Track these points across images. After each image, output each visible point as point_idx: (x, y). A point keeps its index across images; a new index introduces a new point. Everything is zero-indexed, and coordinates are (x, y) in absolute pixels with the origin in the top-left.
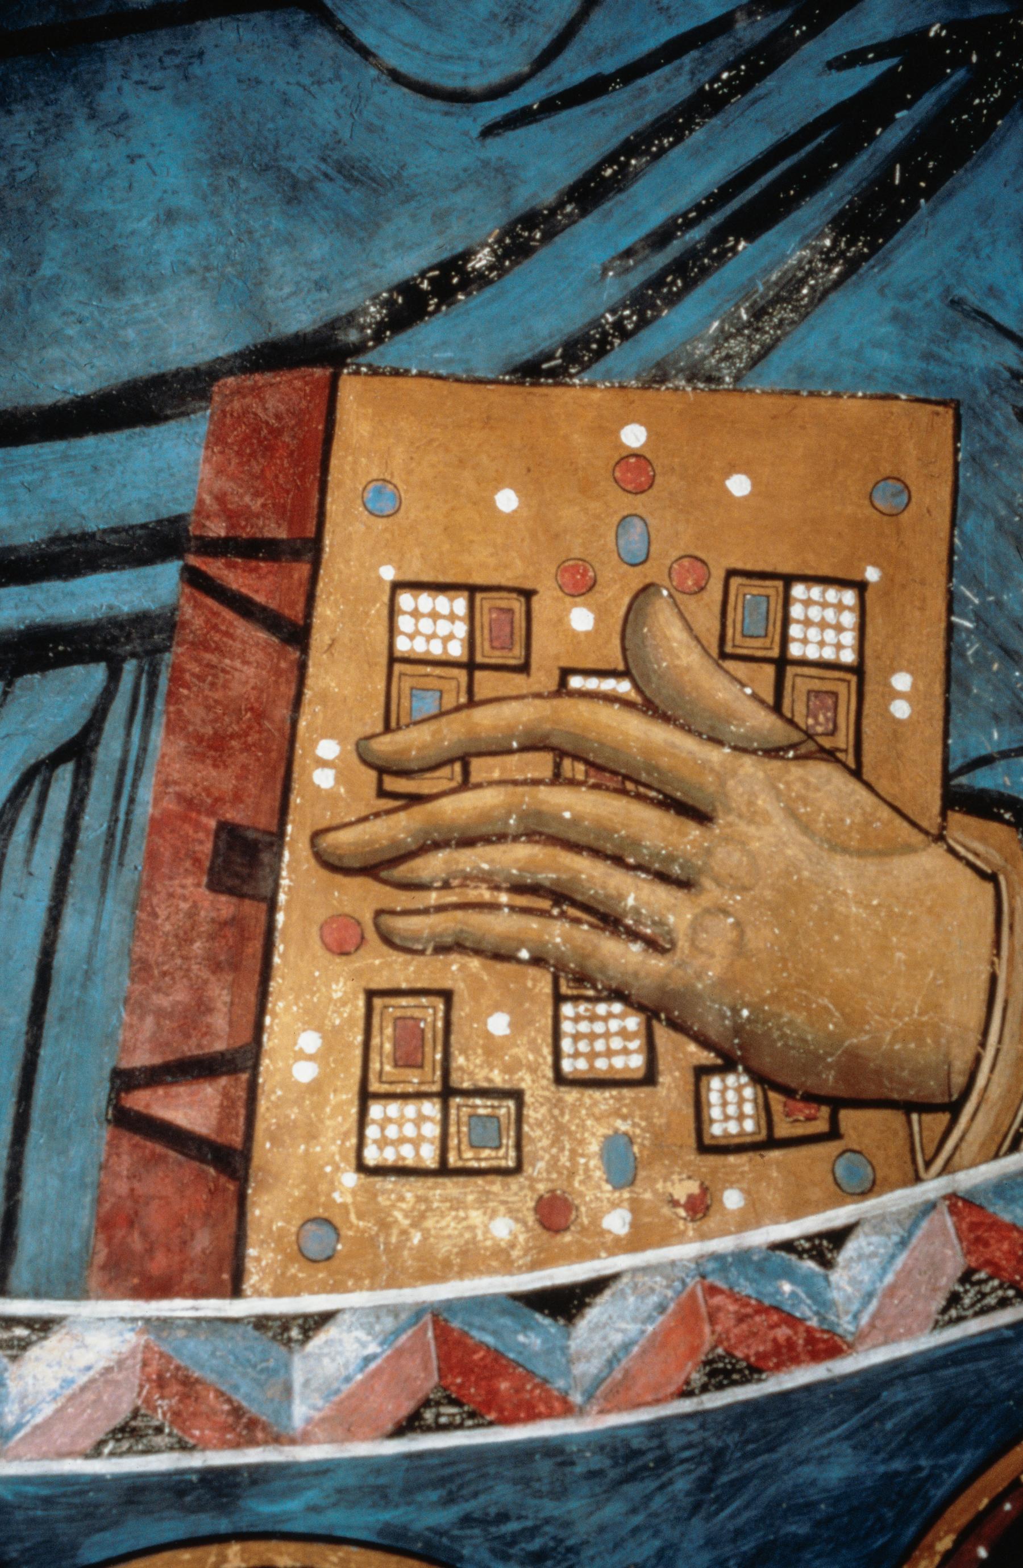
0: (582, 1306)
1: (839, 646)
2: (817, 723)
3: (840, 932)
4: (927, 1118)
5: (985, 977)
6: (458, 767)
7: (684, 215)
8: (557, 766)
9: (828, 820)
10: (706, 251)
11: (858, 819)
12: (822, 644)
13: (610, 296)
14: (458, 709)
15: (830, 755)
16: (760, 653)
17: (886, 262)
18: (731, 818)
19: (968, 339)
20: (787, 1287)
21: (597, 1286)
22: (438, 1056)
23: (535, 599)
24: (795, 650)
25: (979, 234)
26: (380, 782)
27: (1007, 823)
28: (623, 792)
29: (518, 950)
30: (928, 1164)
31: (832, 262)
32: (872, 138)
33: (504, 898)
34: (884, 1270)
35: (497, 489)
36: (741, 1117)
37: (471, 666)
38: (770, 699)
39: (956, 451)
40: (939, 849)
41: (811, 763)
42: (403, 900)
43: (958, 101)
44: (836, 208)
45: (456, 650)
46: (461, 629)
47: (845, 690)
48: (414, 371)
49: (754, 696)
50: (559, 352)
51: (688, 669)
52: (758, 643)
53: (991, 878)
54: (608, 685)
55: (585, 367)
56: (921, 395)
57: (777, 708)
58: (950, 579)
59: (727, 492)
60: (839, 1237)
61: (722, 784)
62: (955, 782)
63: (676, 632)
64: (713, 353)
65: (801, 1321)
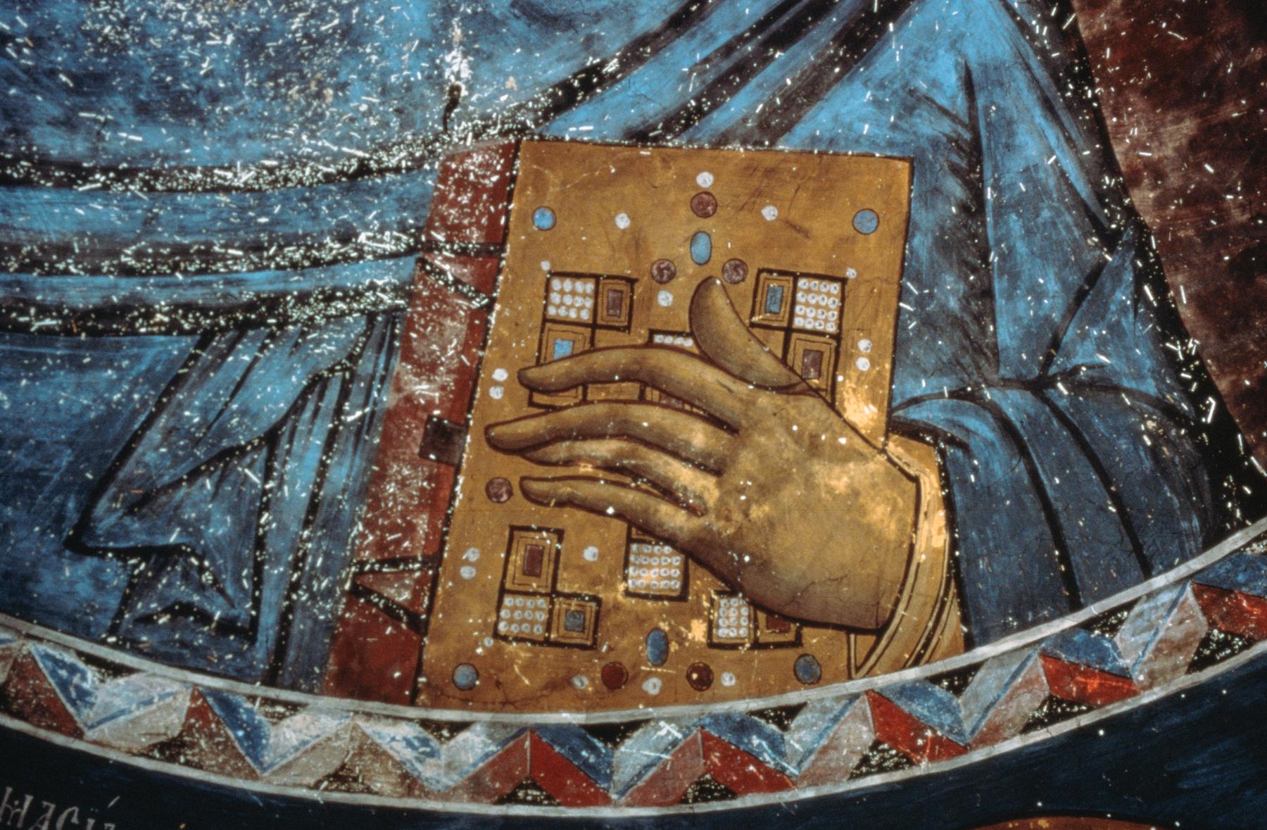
0: (624, 736)
1: (826, 321)
4: (860, 638)
6: (580, 389)
8: (642, 393)
13: (694, 88)
14: (584, 353)
15: (815, 392)
16: (775, 324)
19: (920, 116)
20: (756, 741)
21: (633, 726)
22: (551, 571)
23: (637, 285)
24: (798, 322)
26: (531, 397)
27: (928, 443)
28: (683, 411)
29: (607, 507)
30: (858, 669)
33: (601, 474)
34: (821, 736)
36: (739, 627)
37: (594, 326)
38: (779, 354)
39: (911, 191)
42: (539, 471)
44: (838, 29)
45: (585, 316)
46: (589, 303)
48: (567, 138)
49: (770, 352)
50: (661, 125)
54: (679, 341)
57: (783, 361)
58: (901, 278)
60: (793, 711)
62: (896, 414)
65: (763, 762)
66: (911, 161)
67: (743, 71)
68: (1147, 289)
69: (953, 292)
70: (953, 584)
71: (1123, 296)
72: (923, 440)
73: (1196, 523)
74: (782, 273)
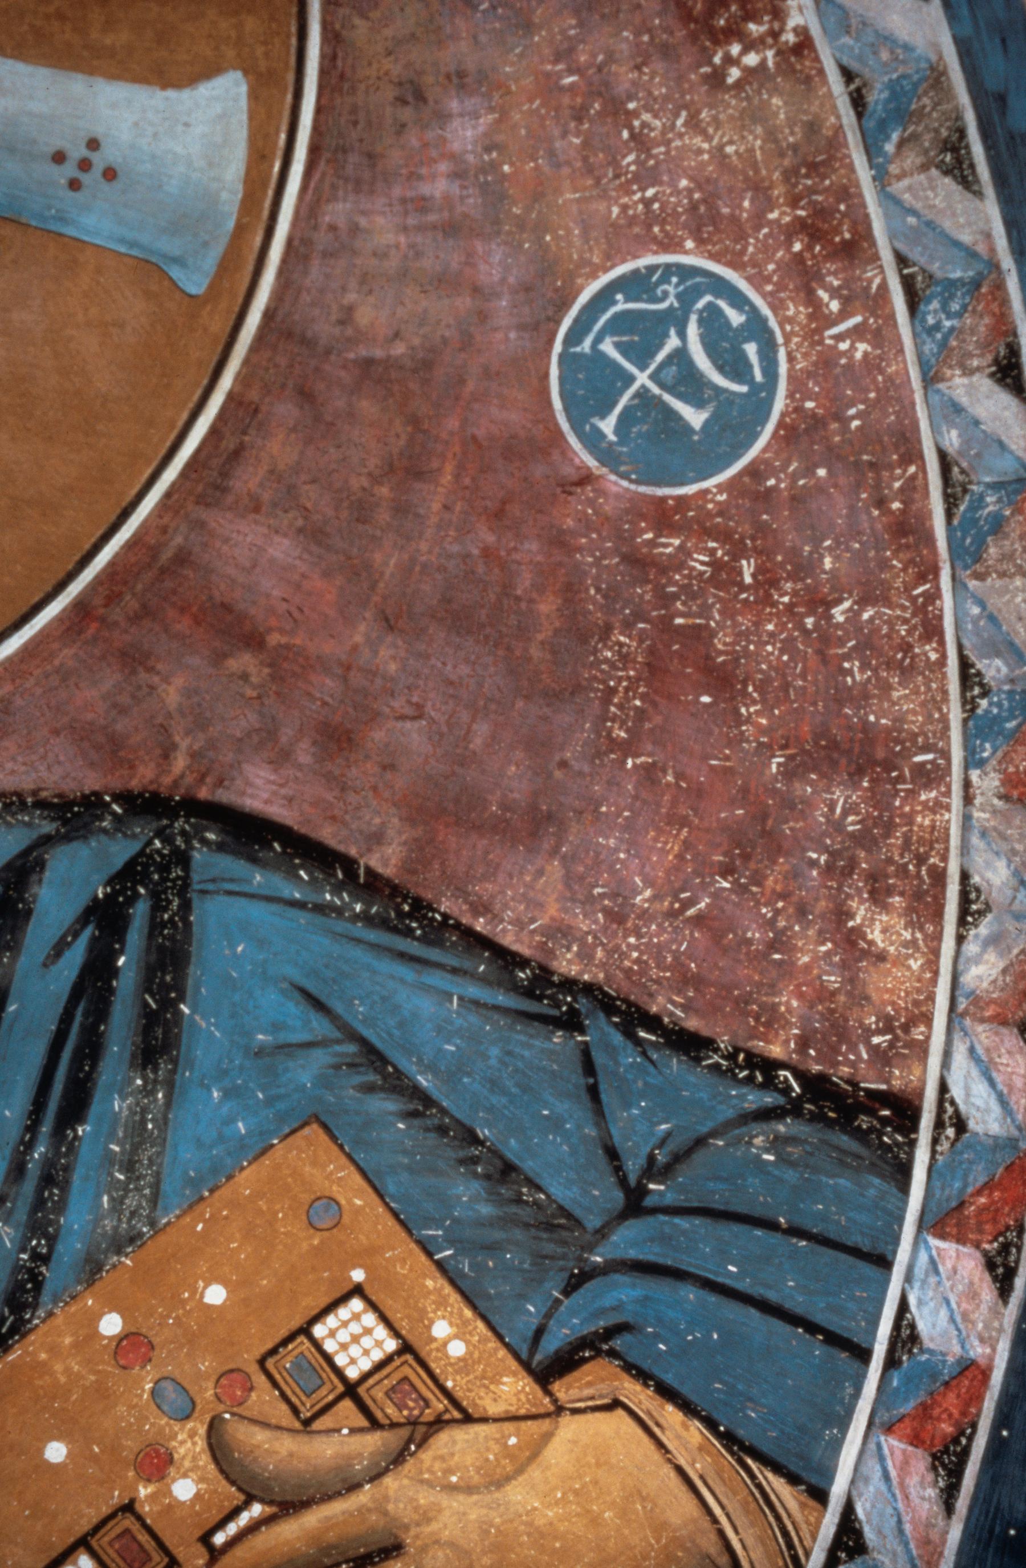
2: (411, 1409)
3: (556, 1538)
5: (673, 1474)
7: (22, 1142)
9: (478, 1470)
10: (58, 1154)
11: (496, 1448)
12: (366, 1352)
15: (439, 1423)
16: (331, 1398)
17: (191, 1065)
18: (413, 1531)
19: (286, 1070)
23: (137, 1506)
25: (237, 998)
27: (591, 1358)
31: (153, 1093)
32: (111, 991)
35: (41, 1451)
38: (364, 1423)
40: (566, 1419)
41: (431, 1441)
43: (155, 926)
44: (127, 1055)
47: (409, 1369)
49: (353, 1431)
50: (6, 1311)
51: (291, 1455)
52: (324, 1391)
53: (616, 1404)
55: (35, 1306)
56: (287, 1130)
57: (375, 1424)
59: (209, 1307)
61: (386, 1513)
63: (260, 1436)
64: (120, 1220)
66: (316, 1118)
67: (54, 1177)
68: (642, 1034)
69: (474, 1199)
70: (749, 1461)
71: (630, 1058)
72: (584, 1361)
73: (877, 1181)
74: (285, 1342)
